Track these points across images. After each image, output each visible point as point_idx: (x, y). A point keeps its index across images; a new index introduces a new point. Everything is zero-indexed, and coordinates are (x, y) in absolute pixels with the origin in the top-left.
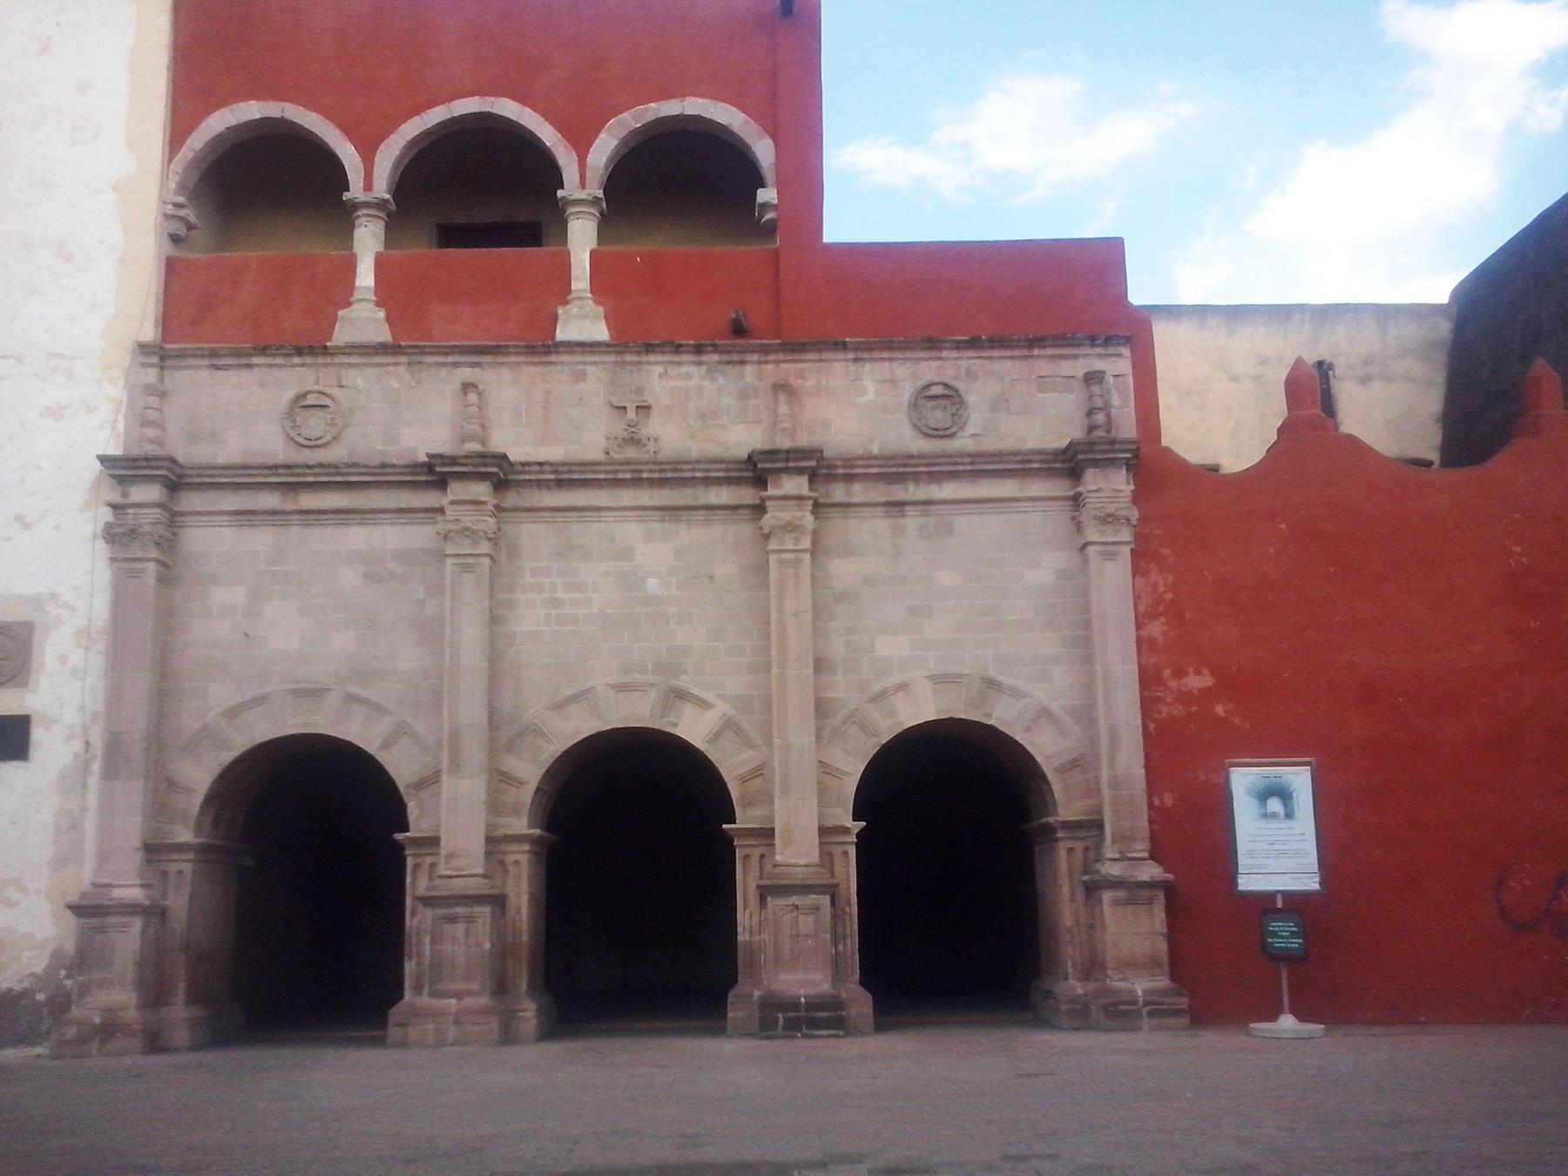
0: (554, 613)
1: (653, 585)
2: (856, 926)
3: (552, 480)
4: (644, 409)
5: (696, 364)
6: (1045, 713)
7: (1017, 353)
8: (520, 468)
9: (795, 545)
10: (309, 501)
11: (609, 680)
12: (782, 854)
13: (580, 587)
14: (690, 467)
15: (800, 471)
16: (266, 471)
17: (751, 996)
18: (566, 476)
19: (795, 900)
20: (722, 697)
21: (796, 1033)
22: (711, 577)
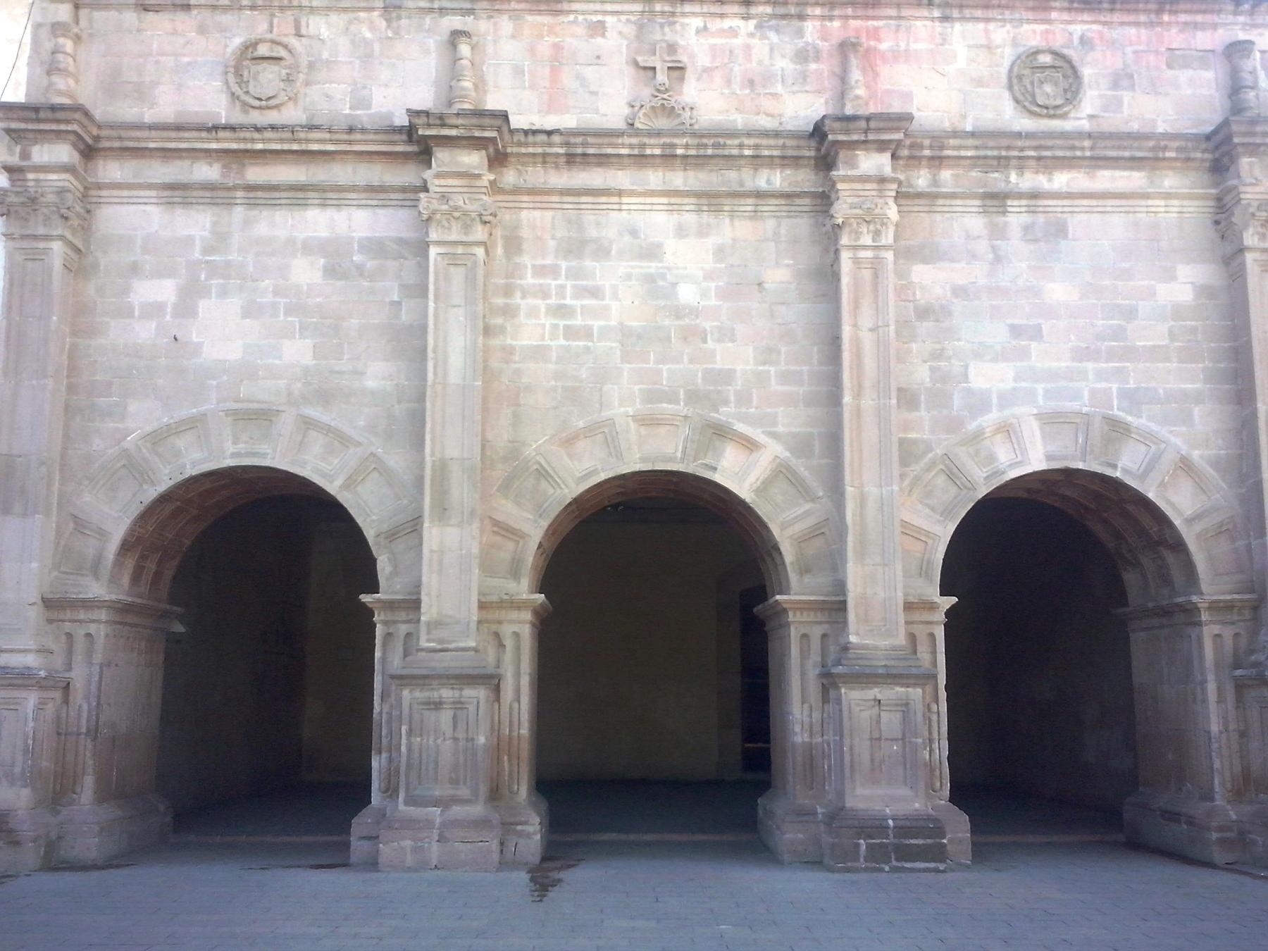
0: (562, 323)
1: (687, 294)
2: (945, 728)
3: (562, 155)
4: (677, 70)
5: (743, 18)
6: (1185, 465)
7: (1143, 18)
8: (522, 139)
9: (874, 240)
10: (256, 174)
11: (631, 411)
12: (858, 634)
13: (595, 293)
14: (737, 142)
15: (882, 146)
16: (204, 134)
17: (815, 814)
18: (579, 151)
19: (875, 692)
20: (774, 435)
21: (883, 866)
22: (759, 284)
